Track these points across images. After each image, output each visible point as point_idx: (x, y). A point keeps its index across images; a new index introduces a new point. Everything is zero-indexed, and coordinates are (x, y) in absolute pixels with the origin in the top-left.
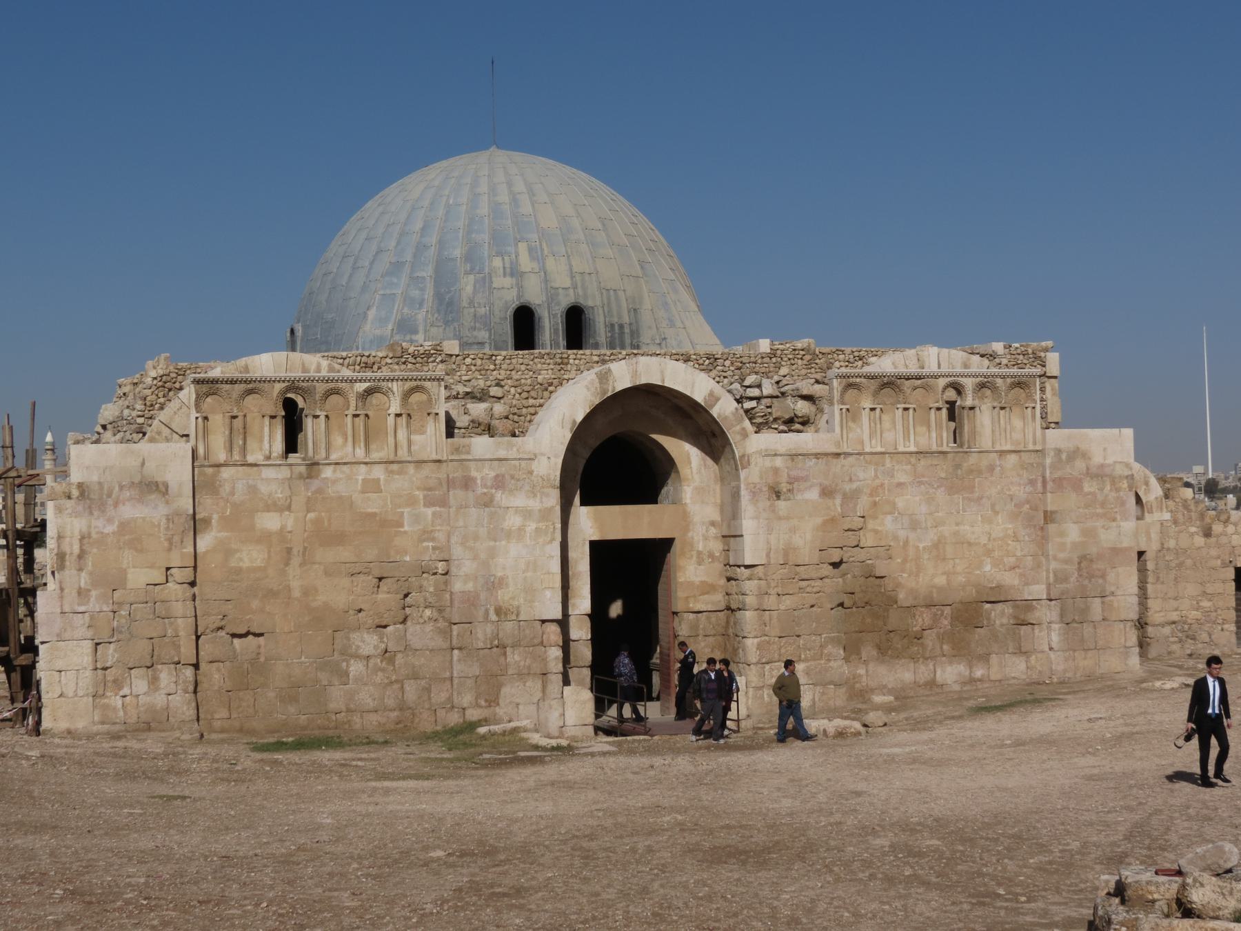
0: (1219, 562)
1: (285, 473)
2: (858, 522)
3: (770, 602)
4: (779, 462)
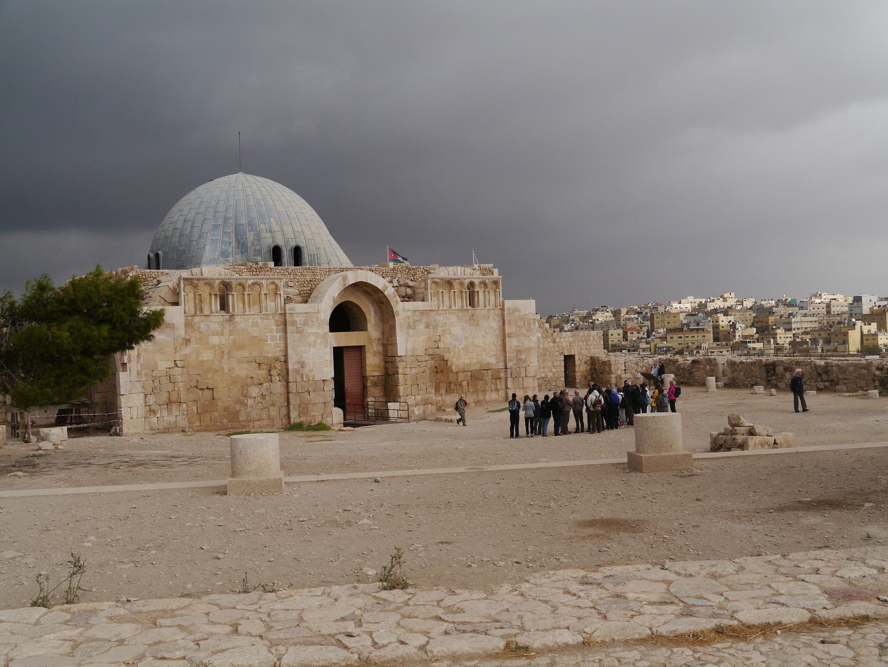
1: (220, 319)
3: (408, 371)
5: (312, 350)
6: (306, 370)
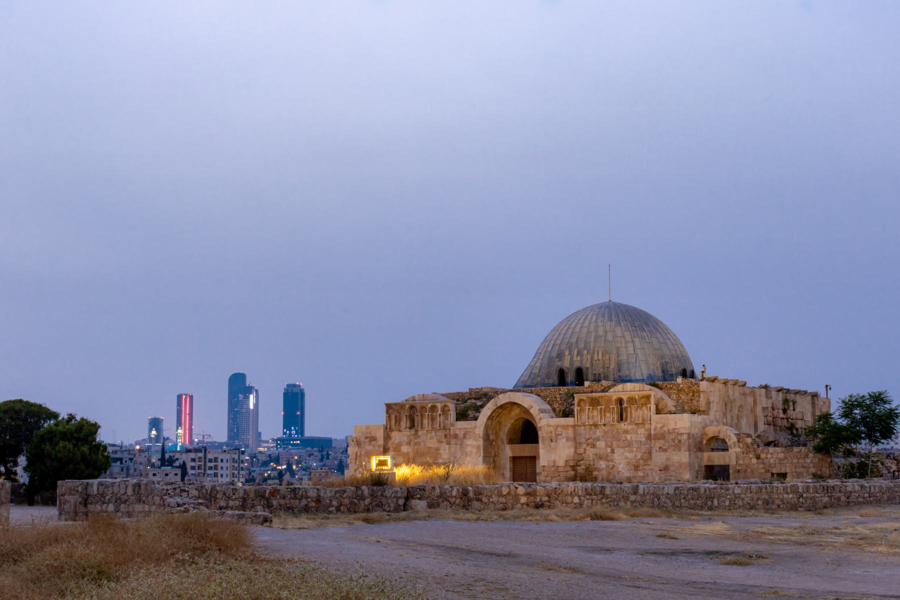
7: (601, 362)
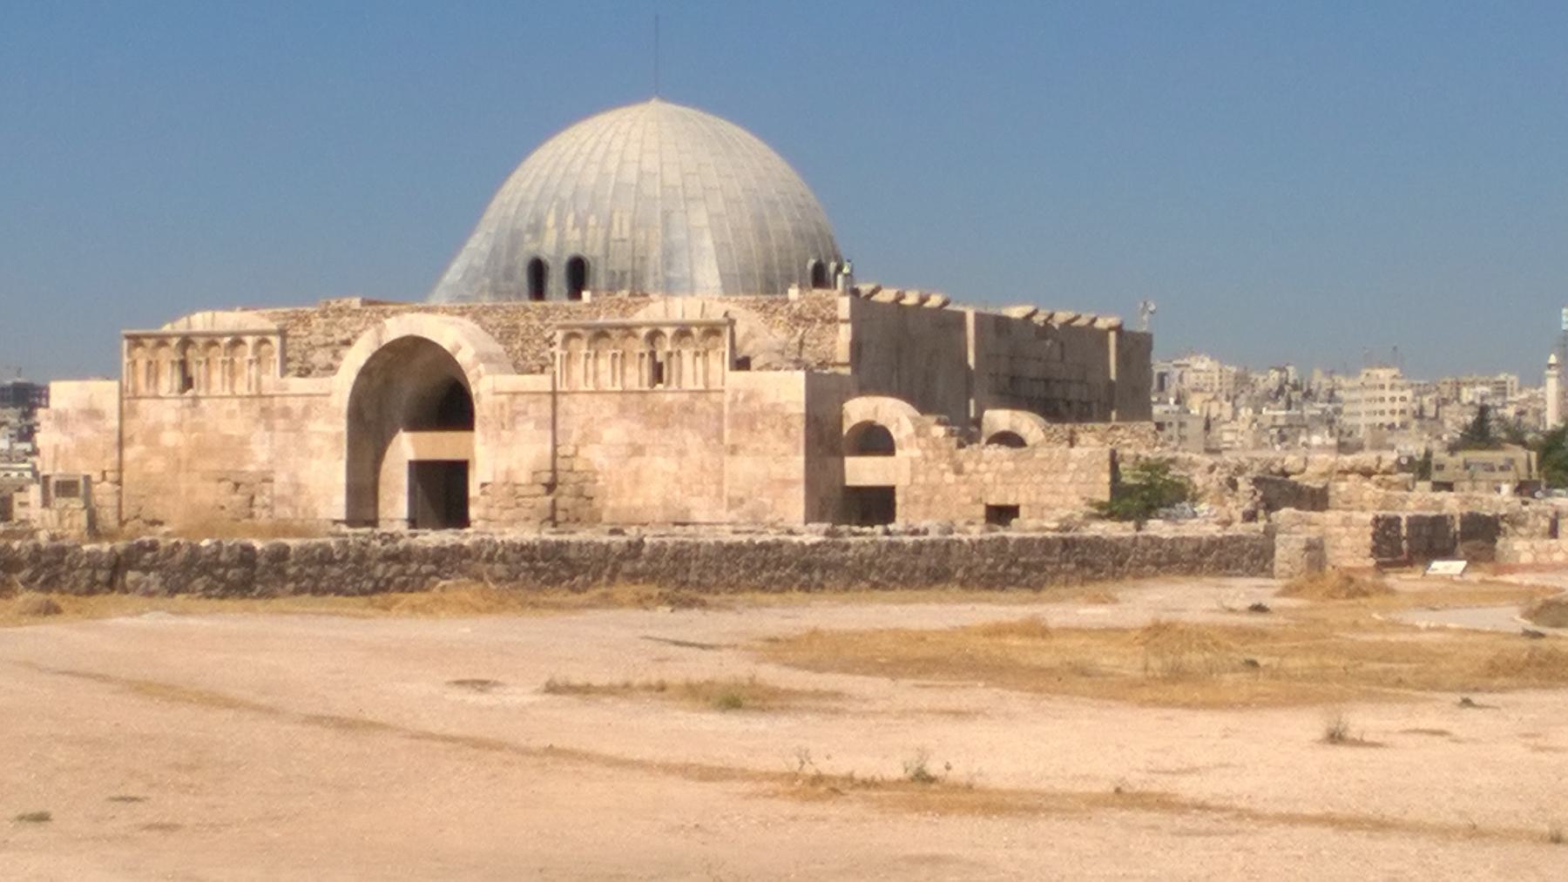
0: (969, 500)
1: (178, 403)
2: (570, 450)
3: (494, 513)
4: (503, 398)
5: (315, 463)
6: (303, 499)
7: (629, 245)
